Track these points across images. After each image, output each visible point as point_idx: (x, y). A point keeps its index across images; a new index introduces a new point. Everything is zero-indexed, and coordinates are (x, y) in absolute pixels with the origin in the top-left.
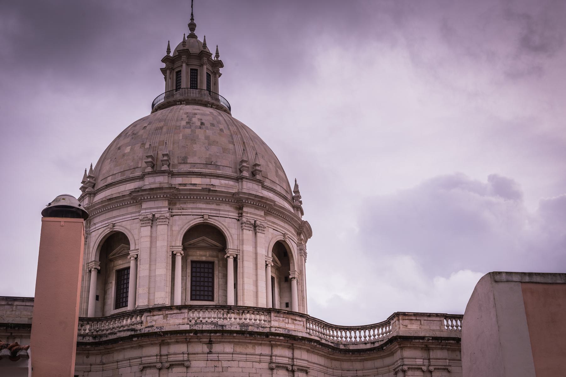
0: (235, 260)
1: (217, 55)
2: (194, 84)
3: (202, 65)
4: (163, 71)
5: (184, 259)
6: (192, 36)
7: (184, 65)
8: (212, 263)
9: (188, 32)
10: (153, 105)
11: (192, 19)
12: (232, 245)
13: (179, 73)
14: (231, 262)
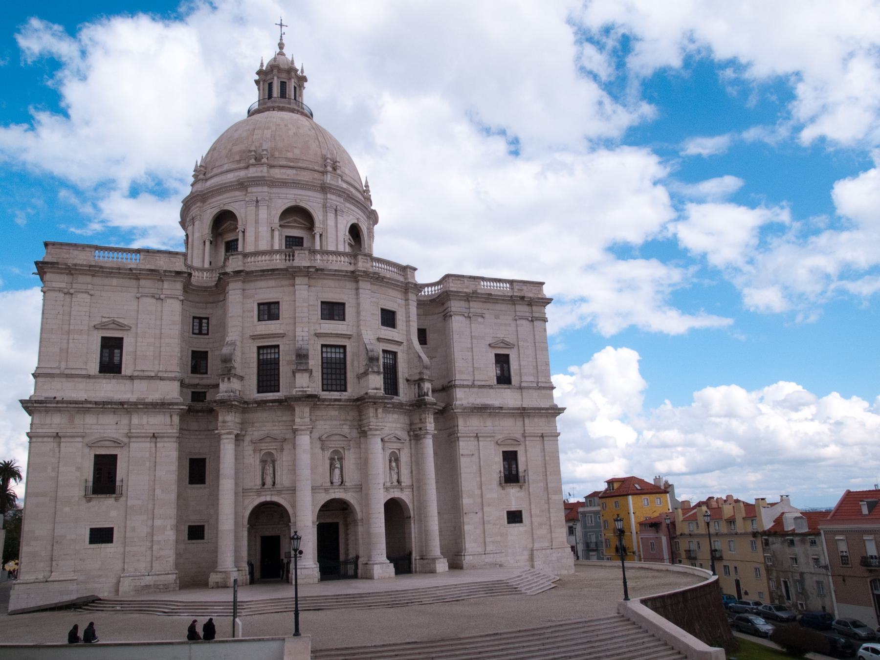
0: (321, 235)
1: (302, 72)
2: (283, 94)
3: (290, 79)
4: (257, 82)
5: (280, 235)
6: (281, 54)
7: (275, 78)
8: (302, 238)
9: (278, 50)
10: (249, 111)
11: (281, 39)
12: (318, 224)
13: (270, 85)
14: (317, 237)
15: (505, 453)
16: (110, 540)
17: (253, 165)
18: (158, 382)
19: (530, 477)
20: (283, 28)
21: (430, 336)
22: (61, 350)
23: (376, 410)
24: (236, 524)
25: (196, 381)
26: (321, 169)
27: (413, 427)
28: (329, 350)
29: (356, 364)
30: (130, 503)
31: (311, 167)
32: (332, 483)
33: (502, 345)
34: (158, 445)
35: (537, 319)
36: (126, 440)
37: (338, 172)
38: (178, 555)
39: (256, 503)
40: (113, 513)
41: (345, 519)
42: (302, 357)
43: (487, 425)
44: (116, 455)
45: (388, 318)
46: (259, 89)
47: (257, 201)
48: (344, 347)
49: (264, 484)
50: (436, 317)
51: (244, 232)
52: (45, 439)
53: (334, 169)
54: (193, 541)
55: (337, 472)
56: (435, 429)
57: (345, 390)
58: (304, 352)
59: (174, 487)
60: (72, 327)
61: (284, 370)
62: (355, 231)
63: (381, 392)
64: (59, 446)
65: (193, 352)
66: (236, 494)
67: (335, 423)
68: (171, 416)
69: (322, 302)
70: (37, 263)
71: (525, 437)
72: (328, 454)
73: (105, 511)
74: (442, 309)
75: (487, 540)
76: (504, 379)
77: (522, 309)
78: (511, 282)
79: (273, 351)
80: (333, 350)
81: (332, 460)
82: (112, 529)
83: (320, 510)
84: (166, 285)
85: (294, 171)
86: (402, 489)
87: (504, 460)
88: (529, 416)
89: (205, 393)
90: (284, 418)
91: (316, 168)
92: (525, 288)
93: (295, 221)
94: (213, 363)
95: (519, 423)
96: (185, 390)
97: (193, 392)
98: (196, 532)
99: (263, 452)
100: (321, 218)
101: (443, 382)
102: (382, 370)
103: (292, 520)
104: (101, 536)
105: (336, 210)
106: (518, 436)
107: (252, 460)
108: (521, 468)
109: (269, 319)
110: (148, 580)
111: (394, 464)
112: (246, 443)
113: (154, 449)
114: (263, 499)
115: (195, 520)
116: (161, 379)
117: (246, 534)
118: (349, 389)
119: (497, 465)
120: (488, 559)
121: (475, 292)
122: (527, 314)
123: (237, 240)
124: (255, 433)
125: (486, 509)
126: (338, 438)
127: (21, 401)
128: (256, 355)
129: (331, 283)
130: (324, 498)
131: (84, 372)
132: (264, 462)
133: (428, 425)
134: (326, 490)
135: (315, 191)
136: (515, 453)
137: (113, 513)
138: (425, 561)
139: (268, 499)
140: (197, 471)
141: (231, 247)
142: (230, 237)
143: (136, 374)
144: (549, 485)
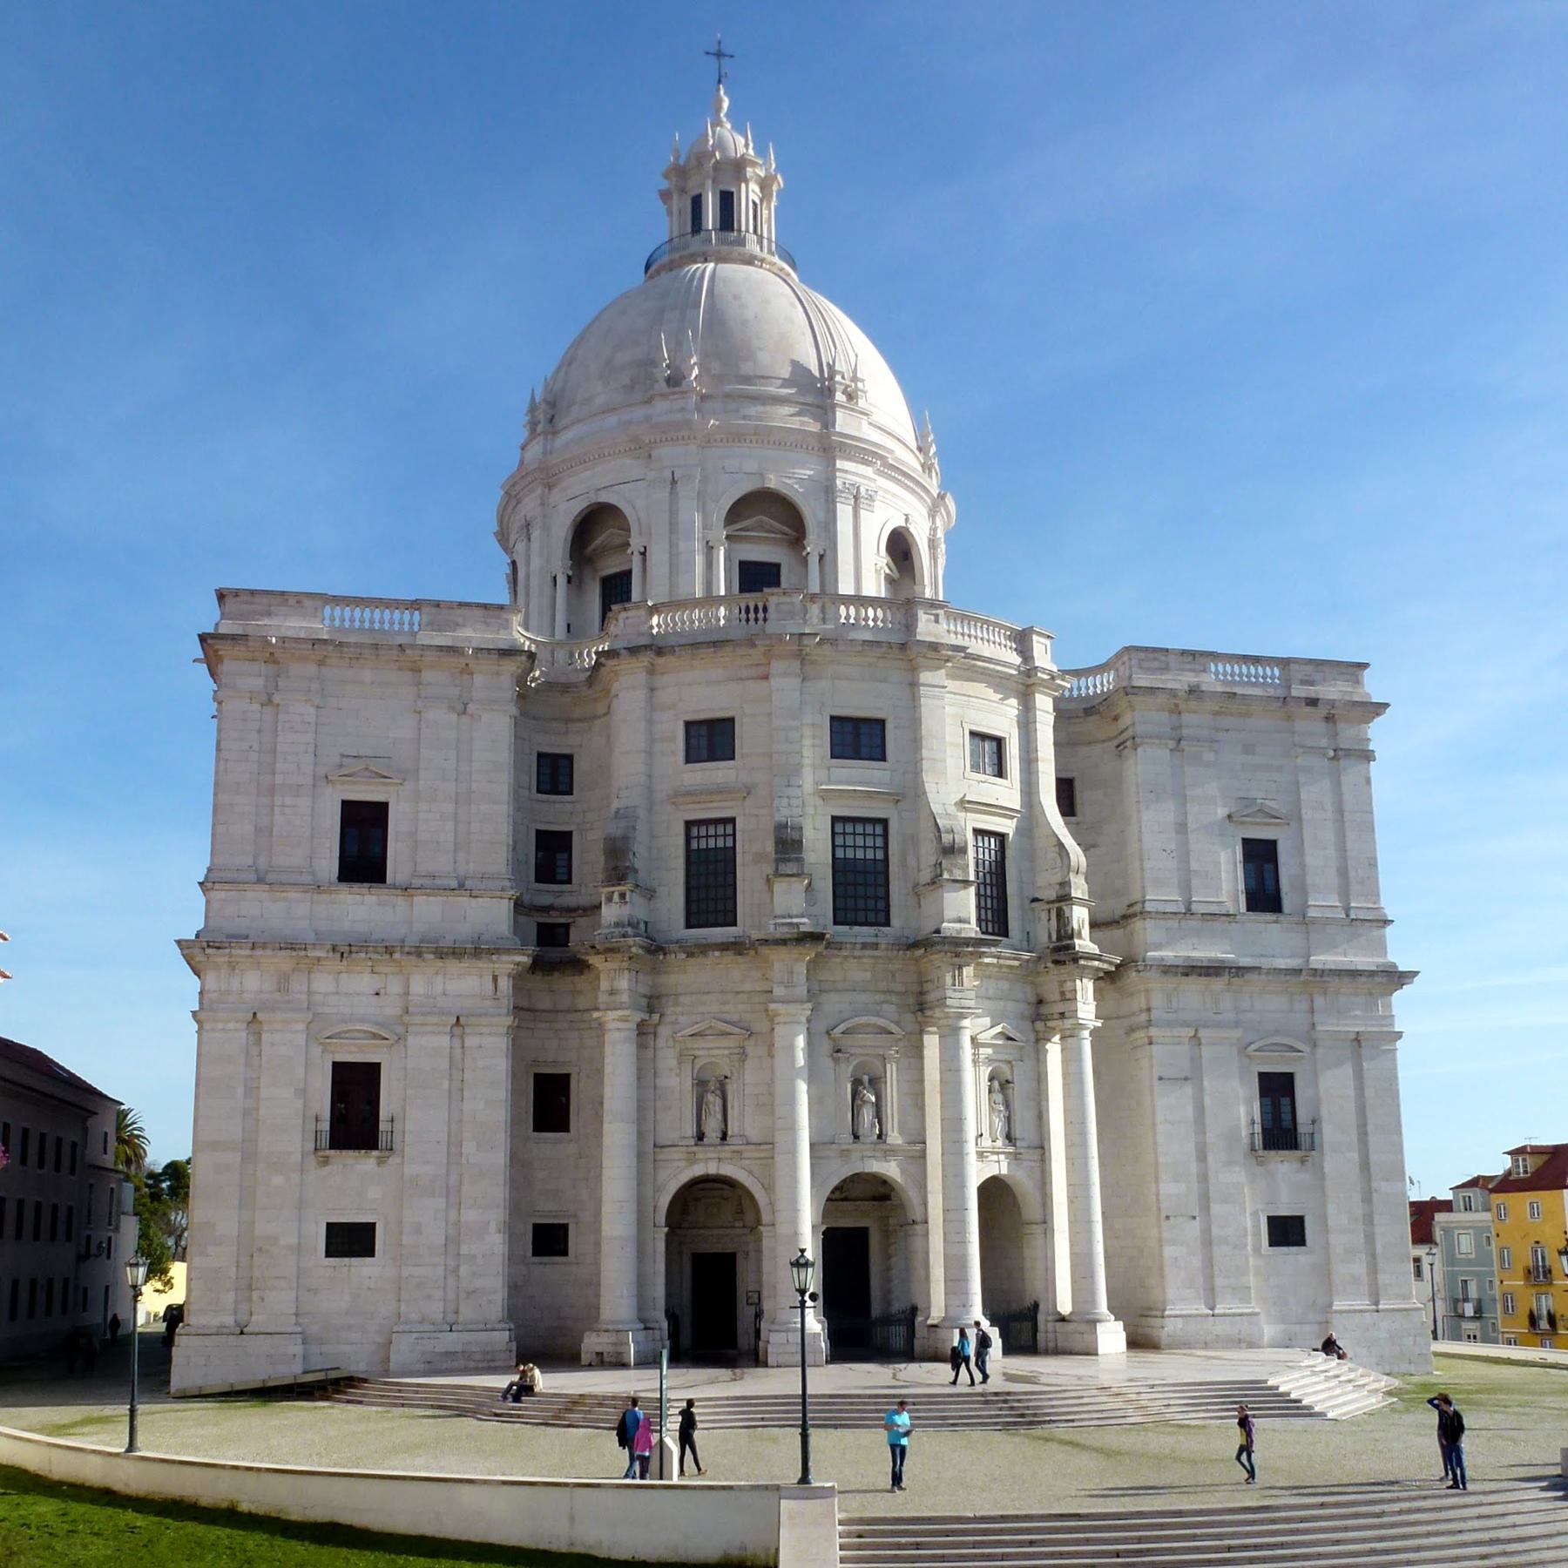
0: (821, 557)
2: (727, 218)
4: (665, 196)
5: (728, 558)
7: (709, 182)
8: (778, 566)
13: (697, 202)
14: (814, 561)
15: (1264, 1078)
16: (369, 1251)
17: (663, 396)
19: (1326, 1139)
20: (725, 61)
21: (1082, 796)
22: (257, 829)
23: (960, 968)
24: (640, 1223)
25: (546, 900)
27: (1044, 1010)
28: (849, 828)
29: (911, 861)
30: (409, 1170)
32: (856, 1137)
34: (469, 1042)
35: (1349, 753)
36: (400, 1030)
37: (861, 403)
38: (514, 1288)
39: (685, 1177)
40: (374, 1192)
41: (884, 1220)
42: (788, 845)
44: (376, 1067)
46: (670, 213)
47: (674, 482)
48: (884, 823)
49: (700, 1136)
50: (1097, 748)
51: (643, 554)
52: (231, 1026)
53: (851, 397)
54: (545, 1259)
55: (867, 1115)
56: (1097, 1017)
57: (887, 924)
58: (796, 836)
59: (502, 1138)
60: (279, 779)
61: (749, 877)
62: (900, 547)
63: (972, 929)
64: (259, 1041)
65: (539, 833)
66: (640, 1156)
67: (862, 998)
68: (495, 979)
69: (833, 718)
70: (203, 638)
72: (847, 1071)
73: (356, 1187)
74: (1112, 730)
75: (1219, 1281)
76: (1264, 894)
77: (1310, 726)
78: (1284, 663)
79: (720, 830)
80: (859, 829)
81: (857, 1083)
82: (374, 1224)
83: (829, 1199)
87: (1264, 1092)
89: (567, 926)
90: (747, 987)
92: (1317, 677)
93: (760, 527)
94: (587, 858)
96: (522, 919)
97: (540, 925)
98: (550, 1240)
99: (699, 1063)
100: (821, 515)
101: (1117, 907)
102: (972, 878)
103: (765, 1218)
104: (351, 1240)
105: (856, 498)
107: (677, 1083)
109: (712, 758)
110: (451, 1341)
111: (999, 1097)
112: (661, 1042)
113: (458, 1051)
114: (698, 1170)
115: (548, 1212)
117: (661, 1246)
118: (895, 921)
120: (1221, 1328)
121: (1194, 691)
122: (1324, 742)
123: (630, 572)
124: (681, 1018)
125: (1215, 1208)
127: (179, 942)
128: (681, 840)
130: (840, 1172)
131: (307, 878)
132: (701, 1085)
133: (1080, 1006)
134: (845, 1154)
136: (1289, 1078)
137: (374, 1192)
138: (1069, 1327)
139: (712, 1169)
140: (550, 1102)
141: (617, 590)
142: (611, 567)
143: (417, 882)
144: (1373, 1157)
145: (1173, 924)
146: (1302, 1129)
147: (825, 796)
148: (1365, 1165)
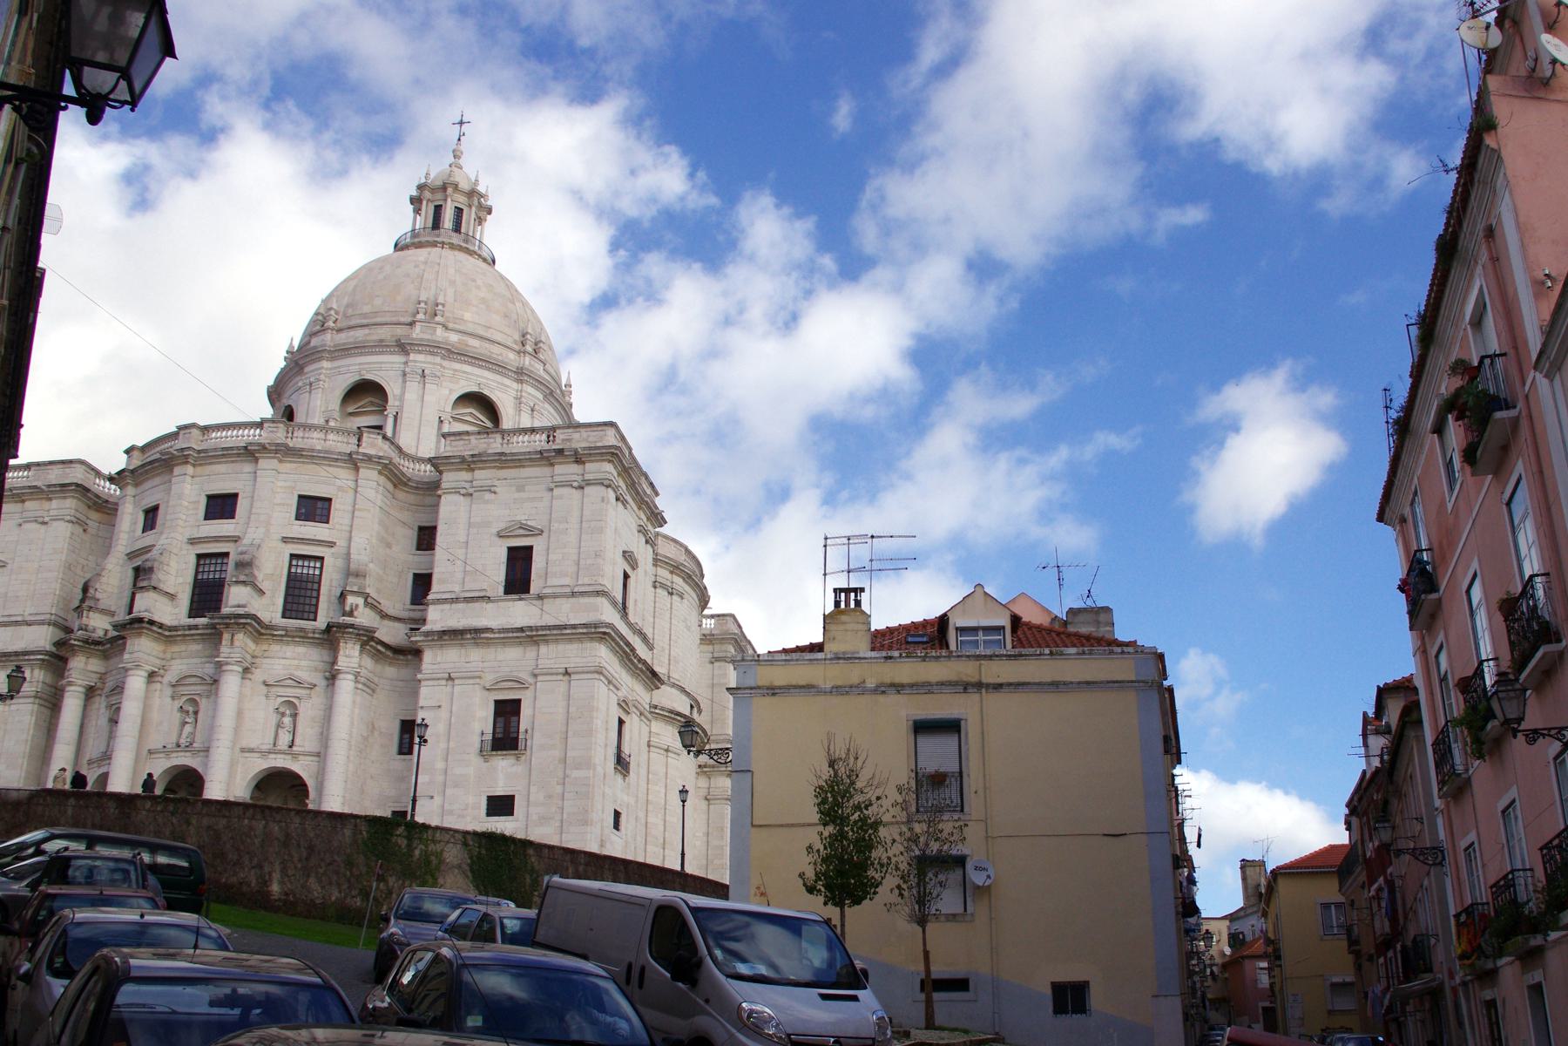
0: (396, 418)
18: (25, 628)
26: (409, 320)
31: (394, 319)
33: (522, 532)
35: (589, 483)
37: (438, 319)
43: (473, 658)
45: (313, 508)
71: (535, 676)
84: (55, 504)
85: (366, 331)
86: (295, 756)
87: (497, 714)
88: (547, 641)
91: (402, 320)
92: (576, 436)
95: (531, 653)
100: (397, 391)
106: (525, 676)
108: (522, 728)
111: (287, 720)
116: (29, 624)
119: (483, 720)
126: (193, 680)
129: (221, 468)
135: (391, 353)
145: (447, 606)
146: (521, 736)
147: (193, 541)
148: (564, 760)
